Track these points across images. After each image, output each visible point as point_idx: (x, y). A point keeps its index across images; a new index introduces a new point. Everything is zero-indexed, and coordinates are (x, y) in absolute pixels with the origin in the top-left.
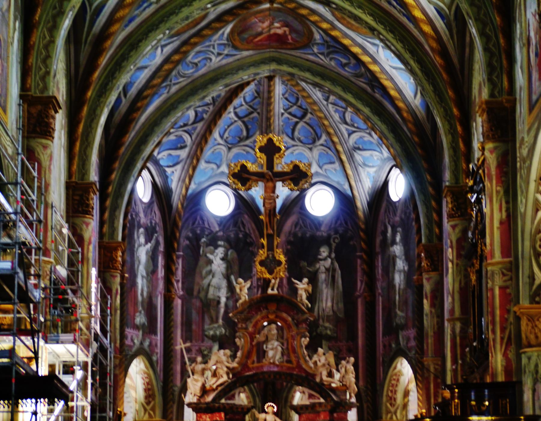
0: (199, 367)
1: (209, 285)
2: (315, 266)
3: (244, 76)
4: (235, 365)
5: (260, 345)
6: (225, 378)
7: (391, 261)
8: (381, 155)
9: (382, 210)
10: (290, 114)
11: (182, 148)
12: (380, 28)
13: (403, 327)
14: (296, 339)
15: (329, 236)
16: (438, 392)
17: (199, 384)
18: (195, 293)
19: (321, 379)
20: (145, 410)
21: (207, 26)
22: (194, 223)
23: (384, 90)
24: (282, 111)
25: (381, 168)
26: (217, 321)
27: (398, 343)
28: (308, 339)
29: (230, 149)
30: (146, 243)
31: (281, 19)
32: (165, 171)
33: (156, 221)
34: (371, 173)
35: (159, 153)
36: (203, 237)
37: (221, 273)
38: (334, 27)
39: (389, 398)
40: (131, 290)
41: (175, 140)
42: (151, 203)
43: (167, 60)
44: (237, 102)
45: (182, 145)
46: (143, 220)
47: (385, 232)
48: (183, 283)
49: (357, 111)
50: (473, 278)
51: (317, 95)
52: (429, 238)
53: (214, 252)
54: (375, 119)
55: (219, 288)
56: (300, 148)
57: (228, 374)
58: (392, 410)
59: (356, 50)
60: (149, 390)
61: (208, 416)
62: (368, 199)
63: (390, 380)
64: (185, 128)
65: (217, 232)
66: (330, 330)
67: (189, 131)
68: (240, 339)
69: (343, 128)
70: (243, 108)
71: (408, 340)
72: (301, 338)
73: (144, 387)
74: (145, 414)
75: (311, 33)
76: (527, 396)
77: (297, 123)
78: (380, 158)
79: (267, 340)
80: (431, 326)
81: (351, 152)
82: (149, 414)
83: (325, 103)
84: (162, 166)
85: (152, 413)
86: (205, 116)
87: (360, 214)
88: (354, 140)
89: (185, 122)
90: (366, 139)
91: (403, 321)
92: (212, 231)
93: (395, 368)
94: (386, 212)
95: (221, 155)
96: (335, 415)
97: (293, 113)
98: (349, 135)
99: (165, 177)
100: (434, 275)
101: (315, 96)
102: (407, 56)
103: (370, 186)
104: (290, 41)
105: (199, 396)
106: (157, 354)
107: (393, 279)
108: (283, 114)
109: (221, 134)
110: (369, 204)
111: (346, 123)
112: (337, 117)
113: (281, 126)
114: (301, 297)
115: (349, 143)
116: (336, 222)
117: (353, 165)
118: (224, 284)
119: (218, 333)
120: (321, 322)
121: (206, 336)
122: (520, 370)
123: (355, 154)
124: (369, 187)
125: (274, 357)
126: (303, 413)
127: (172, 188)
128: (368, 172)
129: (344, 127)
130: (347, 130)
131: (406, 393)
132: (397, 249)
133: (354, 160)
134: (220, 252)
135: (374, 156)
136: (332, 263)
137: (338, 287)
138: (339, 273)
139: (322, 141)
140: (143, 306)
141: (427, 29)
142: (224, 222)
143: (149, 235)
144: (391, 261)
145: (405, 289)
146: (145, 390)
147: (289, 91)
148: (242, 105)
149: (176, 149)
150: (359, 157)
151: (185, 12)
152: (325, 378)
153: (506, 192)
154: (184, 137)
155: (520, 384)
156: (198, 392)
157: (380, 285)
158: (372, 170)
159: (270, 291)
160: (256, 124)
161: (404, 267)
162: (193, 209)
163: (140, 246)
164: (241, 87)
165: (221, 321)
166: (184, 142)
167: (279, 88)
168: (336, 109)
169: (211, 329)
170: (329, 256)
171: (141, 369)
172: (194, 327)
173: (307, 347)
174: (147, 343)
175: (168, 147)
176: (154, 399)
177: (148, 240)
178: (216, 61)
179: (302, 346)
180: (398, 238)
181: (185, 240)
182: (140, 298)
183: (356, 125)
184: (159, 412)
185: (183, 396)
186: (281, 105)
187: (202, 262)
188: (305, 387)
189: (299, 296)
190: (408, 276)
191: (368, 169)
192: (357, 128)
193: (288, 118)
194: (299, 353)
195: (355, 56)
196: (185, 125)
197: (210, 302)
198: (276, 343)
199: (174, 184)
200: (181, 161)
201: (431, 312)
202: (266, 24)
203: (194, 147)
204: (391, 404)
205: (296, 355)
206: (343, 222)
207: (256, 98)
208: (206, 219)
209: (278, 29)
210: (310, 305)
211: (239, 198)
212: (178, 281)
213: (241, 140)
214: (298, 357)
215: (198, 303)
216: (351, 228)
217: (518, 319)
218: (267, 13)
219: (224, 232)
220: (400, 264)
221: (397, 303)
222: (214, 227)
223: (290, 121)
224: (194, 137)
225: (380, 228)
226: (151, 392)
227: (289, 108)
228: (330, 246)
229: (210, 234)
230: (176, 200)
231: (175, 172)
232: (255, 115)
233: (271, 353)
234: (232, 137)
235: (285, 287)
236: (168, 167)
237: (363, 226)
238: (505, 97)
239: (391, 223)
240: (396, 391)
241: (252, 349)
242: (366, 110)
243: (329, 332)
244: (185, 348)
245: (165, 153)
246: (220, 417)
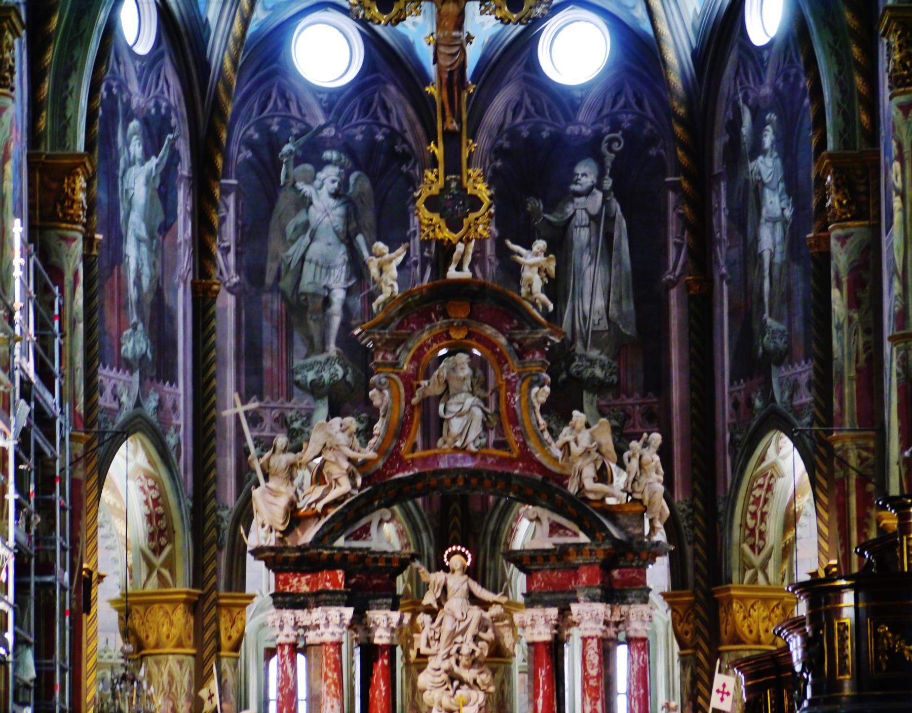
0: (281, 460)
1: (303, 259)
2: (562, 210)
4: (368, 453)
5: (430, 404)
6: (345, 486)
7: (751, 195)
9: (729, 70)
13: (782, 357)
14: (517, 388)
15: (598, 137)
16: (869, 516)
17: (282, 502)
18: (269, 280)
19: (581, 487)
20: (151, 566)
22: (263, 108)
26: (324, 350)
27: (768, 397)
28: (547, 389)
30: (147, 157)
33: (168, 101)
36: (288, 142)
37: (331, 230)
39: (747, 532)
40: (112, 273)
42: (155, 57)
46: (137, 100)
47: (735, 125)
48: (238, 255)
53: (314, 178)
55: (328, 268)
57: (351, 476)
58: (757, 560)
60: (159, 517)
61: (303, 579)
63: (750, 490)
65: (321, 128)
66: (602, 367)
68: (381, 390)
71: (795, 388)
72: (531, 386)
73: (146, 510)
74: (149, 576)
79: (446, 394)
80: (850, 353)
82: (160, 576)
85: (166, 573)
87: (675, 79)
91: (781, 343)
92: (309, 127)
93: (762, 459)
94: (737, 73)
96: (616, 573)
100: (856, 227)
103: (698, 11)
105: (281, 532)
106: (177, 428)
107: (757, 240)
110: (694, 53)
114: (530, 286)
116: (615, 103)
118: (340, 255)
119: (326, 376)
120: (579, 347)
121: (297, 383)
124: (695, 10)
125: (465, 432)
126: (537, 571)
127: (207, 20)
131: (791, 520)
134: (330, 175)
136: (605, 202)
137: (620, 262)
138: (621, 225)
140: (140, 312)
145: (786, 264)
146: (149, 517)
152: (589, 484)
156: (280, 523)
159: (452, 273)
161: (783, 209)
162: (261, 73)
163: (130, 164)
165: (332, 349)
169: (311, 367)
170: (599, 185)
171: (138, 468)
172: (267, 363)
173: (545, 409)
174: (151, 404)
176: (171, 540)
177: (151, 149)
179: (534, 408)
180: (768, 139)
181: (243, 148)
182: (133, 293)
184: (183, 570)
185: (242, 531)
187: (284, 200)
188: (542, 506)
189: (523, 283)
194: (526, 423)
197: (306, 300)
198: (470, 400)
201: (850, 320)
204: (752, 547)
205: (518, 428)
206: (633, 101)
208: (293, 97)
210: (551, 307)
211: (372, 41)
212: (226, 250)
214: (522, 433)
215: (276, 304)
216: (651, 115)
219: (337, 128)
221: (766, 299)
222: (314, 117)
225: (723, 114)
226: (163, 524)
228: (600, 160)
229: (303, 133)
233: (456, 425)
235: (491, 263)
237: (681, 111)
239: (750, 101)
240: (764, 514)
241: (412, 415)
243: (599, 372)
244: (246, 413)
246: (335, 583)
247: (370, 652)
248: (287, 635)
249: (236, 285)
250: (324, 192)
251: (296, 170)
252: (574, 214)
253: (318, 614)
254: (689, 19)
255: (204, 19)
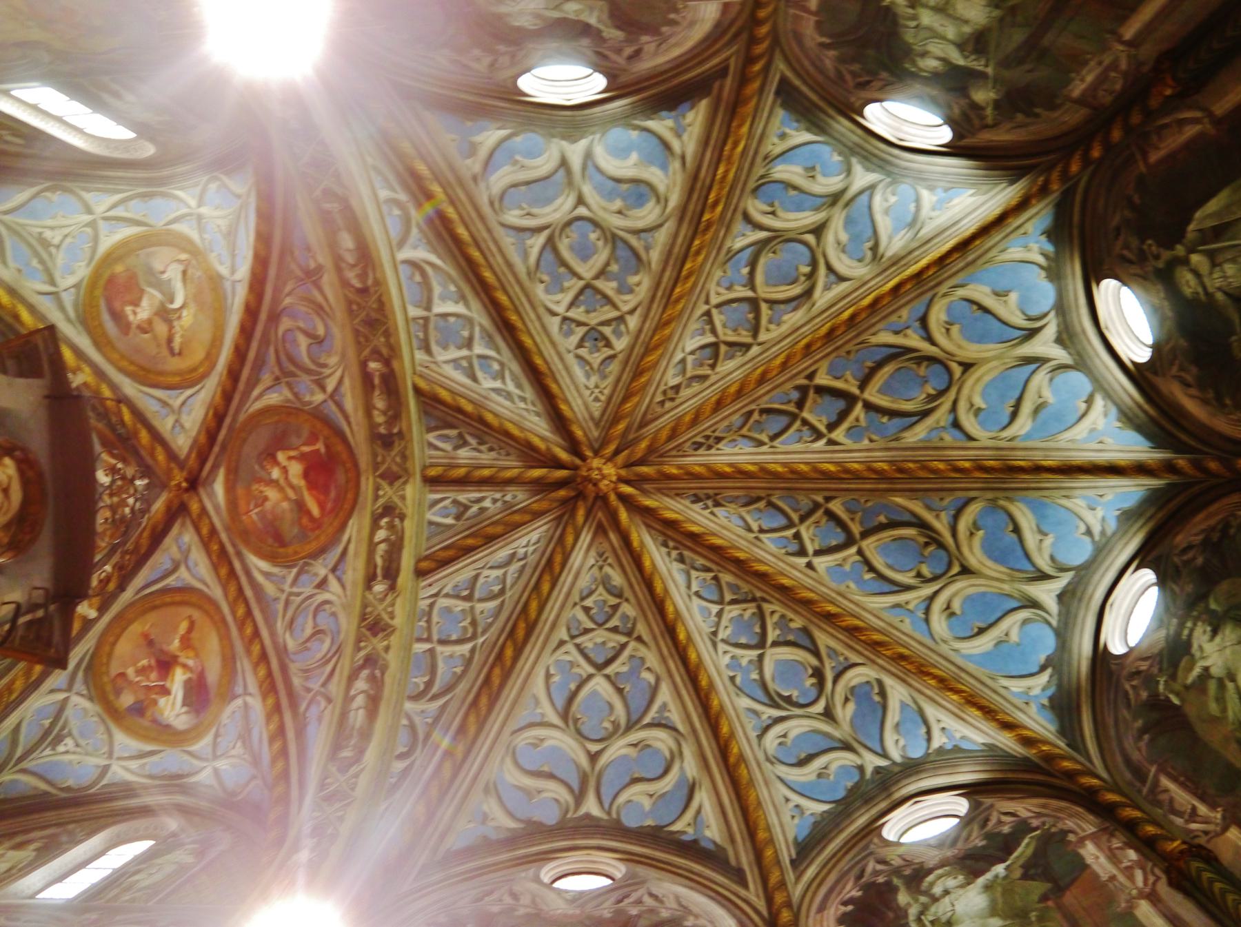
8: (880, 186)
10: (832, 427)
11: (883, 693)
24: (820, 444)
25: (920, 178)
29: (966, 571)
31: (257, 467)
32: (941, 751)
34: (934, 198)
35: (885, 755)
41: (858, 704)
45: (876, 690)
48: (1202, 798)
56: (965, 391)
62: (1004, 185)
64: (829, 676)
67: (841, 668)
69: (822, 298)
70: (805, 535)
77: (868, 406)
78: (889, 190)
81: (885, 266)
83: (755, 350)
84: (927, 755)
86: (797, 623)
88: (855, 264)
89: (810, 671)
90: (844, 237)
95: (984, 594)
97: (834, 418)
98: (842, 279)
101: (735, 374)
103: (971, 191)
104: (320, 446)
108: (831, 442)
109: (585, 594)
111: (808, 293)
112: (793, 318)
113: (872, 445)
115: (865, 274)
117: (917, 253)
123: (889, 254)
127: (983, 744)
128: (933, 209)
129: (820, 297)
130: (827, 288)
133: (903, 253)
135: (889, 204)
137: (1228, 208)
139: (913, 340)
147: (744, 431)
148: (797, 536)
149: (884, 707)
154: (854, 683)
158: (927, 197)
160: (869, 504)
166: (868, 682)
168: (770, 321)
175: (875, 731)
183: (807, 270)
186: (798, 447)
191: (925, 211)
192: (814, 264)
193: (850, 428)
196: (818, 674)
200: (915, 702)
202: (272, 494)
203: (880, 661)
207: (770, 504)
218: (240, 491)
223: (863, 423)
224: (855, 658)
227: (813, 429)
231: (943, 725)
232: (836, 506)
234: (922, 562)
236: (929, 739)
245: (890, 738)
249: (1224, 818)
250: (1209, 648)
251: (1179, 680)
252: (1219, 289)
254: (981, 199)
255: (983, 748)
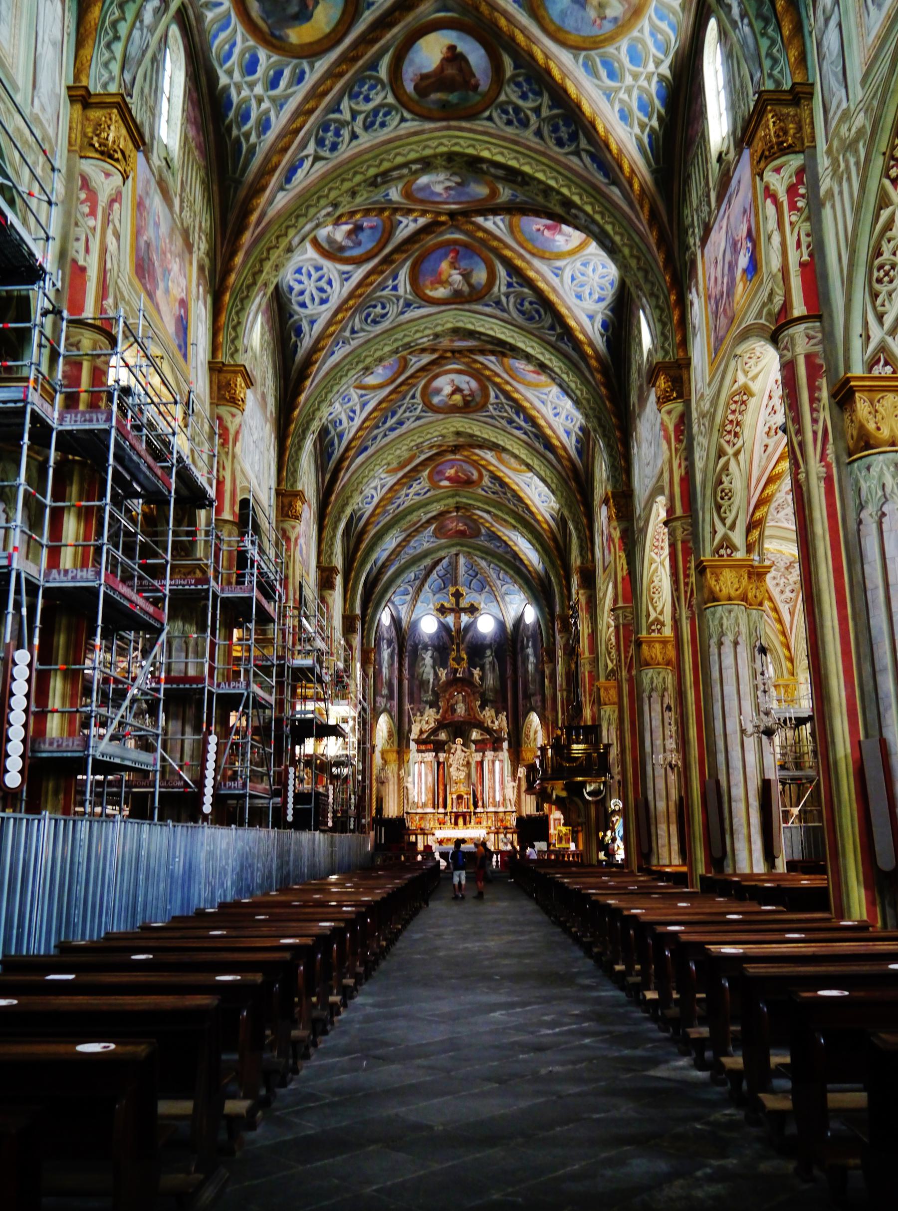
3: (442, 554)
4: (438, 717)
6: (433, 725)
12: (518, 526)
13: (534, 695)
21: (422, 526)
23: (521, 560)
38: (493, 526)
42: (390, 626)
43: (399, 545)
44: (438, 568)
46: (386, 635)
49: (506, 573)
50: (573, 666)
51: (483, 564)
52: (548, 644)
54: (517, 577)
59: (505, 538)
69: (498, 582)
75: (480, 530)
76: (604, 733)
79: (457, 703)
99: (398, 611)
100: (551, 665)
102: (534, 541)
112: (495, 576)
118: (432, 671)
122: (600, 718)
131: (536, 732)
132: (530, 651)
141: (545, 526)
142: (431, 637)
143: (390, 643)
144: (526, 658)
150: (507, 598)
151: (409, 518)
153: (591, 618)
155: (600, 726)
157: (520, 672)
164: (441, 560)
167: (462, 560)
177: (389, 646)
178: (426, 546)
184: (396, 744)
190: (536, 666)
195: (505, 542)
199: (403, 615)
209: (461, 527)
211: (440, 623)
213: (441, 589)
217: (599, 689)
220: (532, 659)
225: (520, 639)
230: (404, 624)
238: (589, 565)
242: (511, 572)
247: (439, 763)
248: (420, 759)
253: (427, 754)
